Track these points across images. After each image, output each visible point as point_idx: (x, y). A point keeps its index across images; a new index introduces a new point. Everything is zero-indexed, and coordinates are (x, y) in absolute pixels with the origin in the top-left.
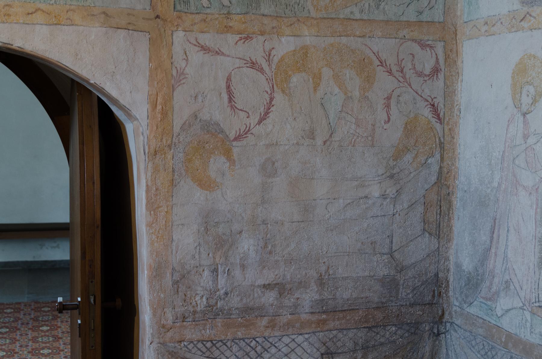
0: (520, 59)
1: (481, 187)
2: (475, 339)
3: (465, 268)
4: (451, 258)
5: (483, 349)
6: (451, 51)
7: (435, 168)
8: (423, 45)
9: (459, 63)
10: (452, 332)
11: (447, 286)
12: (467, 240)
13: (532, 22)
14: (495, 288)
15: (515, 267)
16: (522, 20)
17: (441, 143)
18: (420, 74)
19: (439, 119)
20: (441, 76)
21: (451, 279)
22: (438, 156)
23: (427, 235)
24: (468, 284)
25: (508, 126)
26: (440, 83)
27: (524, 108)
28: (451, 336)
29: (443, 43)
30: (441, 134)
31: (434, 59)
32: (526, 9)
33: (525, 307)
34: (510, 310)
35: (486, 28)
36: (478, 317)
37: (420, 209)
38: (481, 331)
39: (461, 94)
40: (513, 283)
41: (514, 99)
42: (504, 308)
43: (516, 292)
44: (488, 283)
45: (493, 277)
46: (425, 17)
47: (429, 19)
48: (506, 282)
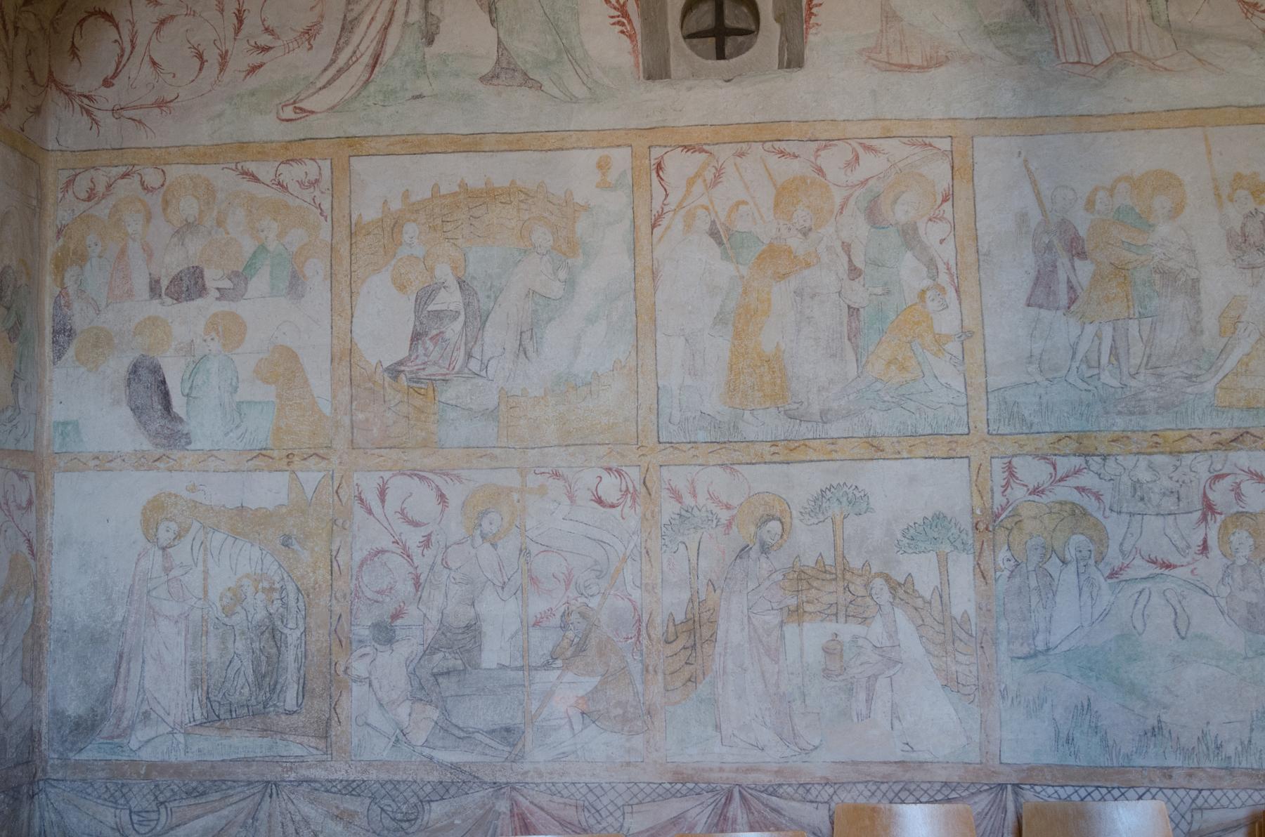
0: (154, 497)
1: (93, 624)
2: (92, 785)
3: (70, 713)
4: (43, 707)
5: (106, 791)
6: (40, 482)
7: (31, 609)
8: (22, 477)
9: (48, 494)
10: (49, 789)
11: (40, 740)
12: (72, 682)
13: (170, 464)
14: (127, 723)
15: (156, 695)
16: (155, 461)
17: (35, 581)
18: (19, 507)
19: (33, 555)
20: (33, 508)
21: (44, 730)
22: (33, 595)
23: (25, 684)
24: (76, 730)
25: (138, 560)
26: (32, 516)
27: (163, 542)
28: (47, 795)
29: (33, 474)
30: (35, 572)
31: (28, 491)
32: (161, 451)
33: (175, 731)
34: (153, 739)
35: (92, 463)
36: (96, 760)
37: (20, 654)
38: (101, 774)
39: (51, 527)
40: (154, 711)
41: (146, 535)
42: (142, 739)
43: (160, 719)
44: (113, 721)
45: (124, 712)
46: (21, 446)
47: (24, 448)
48: (146, 712)
